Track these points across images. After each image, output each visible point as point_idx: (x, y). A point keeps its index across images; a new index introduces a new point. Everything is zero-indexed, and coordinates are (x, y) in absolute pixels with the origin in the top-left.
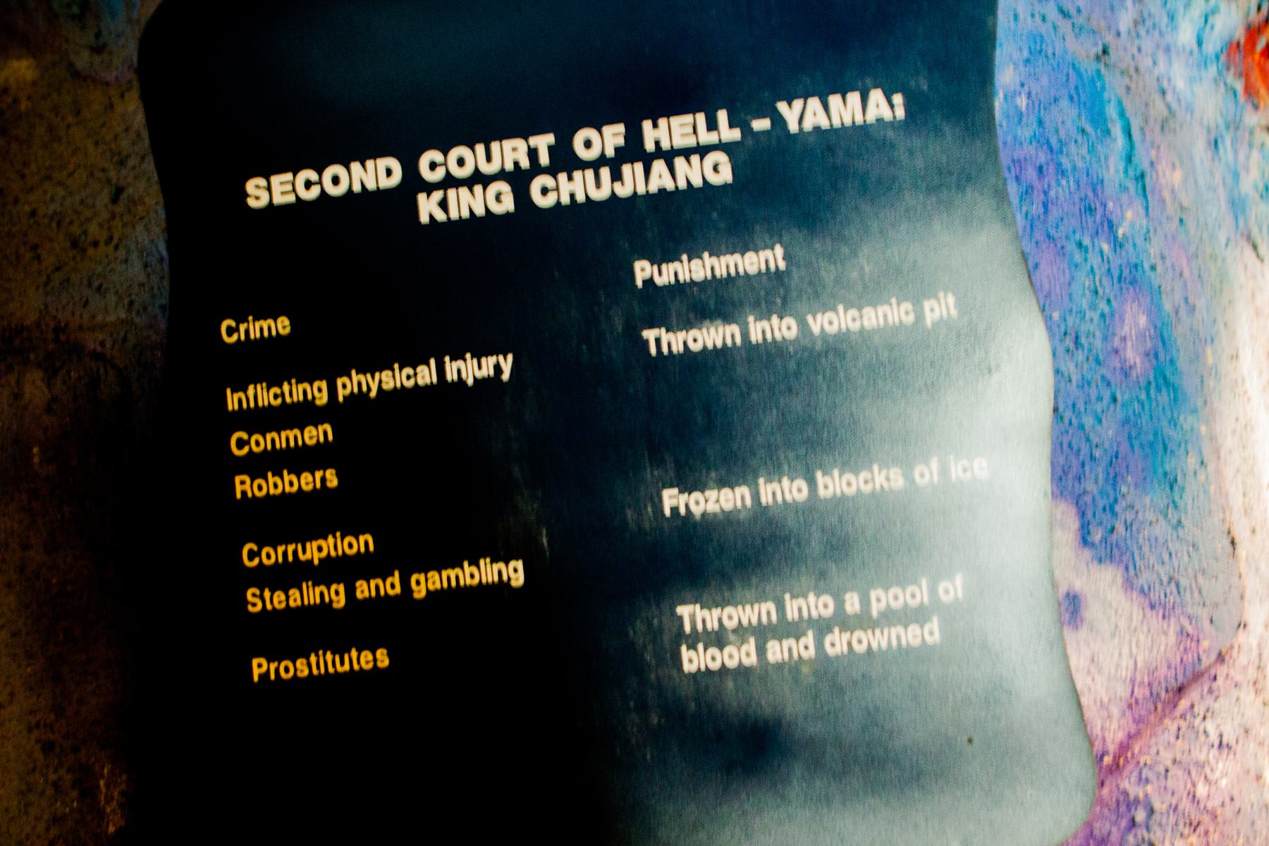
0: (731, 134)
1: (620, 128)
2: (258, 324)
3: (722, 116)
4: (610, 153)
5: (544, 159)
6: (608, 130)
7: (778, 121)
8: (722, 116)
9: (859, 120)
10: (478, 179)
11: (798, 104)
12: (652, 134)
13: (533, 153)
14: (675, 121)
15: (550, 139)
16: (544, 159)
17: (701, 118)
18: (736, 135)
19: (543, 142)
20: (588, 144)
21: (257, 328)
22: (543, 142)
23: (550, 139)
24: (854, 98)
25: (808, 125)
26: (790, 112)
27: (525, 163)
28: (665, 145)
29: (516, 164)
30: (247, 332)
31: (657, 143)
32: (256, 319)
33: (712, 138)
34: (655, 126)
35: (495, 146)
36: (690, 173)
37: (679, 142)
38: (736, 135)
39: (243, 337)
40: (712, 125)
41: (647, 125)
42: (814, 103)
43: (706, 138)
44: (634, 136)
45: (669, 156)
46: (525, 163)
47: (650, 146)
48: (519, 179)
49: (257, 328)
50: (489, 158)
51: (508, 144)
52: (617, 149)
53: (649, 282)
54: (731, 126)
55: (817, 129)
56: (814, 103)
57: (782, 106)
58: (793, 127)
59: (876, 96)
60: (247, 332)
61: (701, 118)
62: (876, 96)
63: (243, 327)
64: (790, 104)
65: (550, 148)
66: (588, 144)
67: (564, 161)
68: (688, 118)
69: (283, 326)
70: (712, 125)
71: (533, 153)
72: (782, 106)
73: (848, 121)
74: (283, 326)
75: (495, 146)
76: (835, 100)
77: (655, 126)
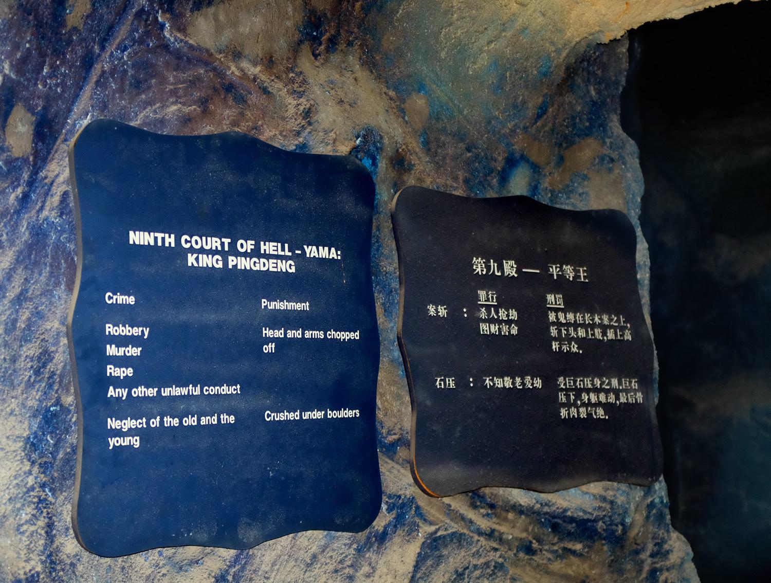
1: (253, 242)
4: (249, 251)
5: (226, 249)
6: (249, 242)
7: (304, 252)
13: (222, 244)
14: (272, 244)
15: (229, 240)
16: (226, 249)
17: (279, 245)
19: (227, 241)
22: (227, 241)
23: (229, 240)
24: (326, 249)
25: (312, 256)
27: (219, 248)
31: (265, 250)
33: (283, 253)
38: (290, 254)
40: (283, 250)
42: (314, 248)
44: (257, 247)
47: (262, 252)
51: (214, 239)
52: (251, 249)
54: (289, 251)
66: (242, 246)
68: (275, 244)
70: (283, 250)
71: (222, 244)
72: (305, 247)
76: (321, 248)
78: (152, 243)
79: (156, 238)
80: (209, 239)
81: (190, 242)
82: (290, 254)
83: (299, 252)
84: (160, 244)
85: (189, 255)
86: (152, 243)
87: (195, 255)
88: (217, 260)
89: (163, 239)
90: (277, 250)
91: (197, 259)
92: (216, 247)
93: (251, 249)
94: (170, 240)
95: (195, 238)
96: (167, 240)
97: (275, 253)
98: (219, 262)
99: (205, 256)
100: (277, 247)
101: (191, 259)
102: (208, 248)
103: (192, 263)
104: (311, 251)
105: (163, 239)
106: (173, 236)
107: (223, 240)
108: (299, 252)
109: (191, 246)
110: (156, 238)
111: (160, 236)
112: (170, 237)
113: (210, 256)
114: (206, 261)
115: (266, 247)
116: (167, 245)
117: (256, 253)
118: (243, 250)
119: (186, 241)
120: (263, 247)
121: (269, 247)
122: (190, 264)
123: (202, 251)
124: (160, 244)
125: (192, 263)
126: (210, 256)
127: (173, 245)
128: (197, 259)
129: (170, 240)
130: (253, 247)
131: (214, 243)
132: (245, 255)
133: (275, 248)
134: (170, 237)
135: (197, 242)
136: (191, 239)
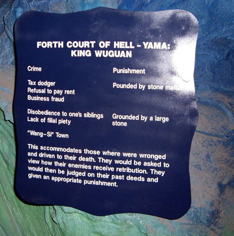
0: (132, 47)
1: (109, 42)
2: (35, 68)
3: (131, 43)
4: (106, 47)
5: (93, 46)
6: (107, 42)
7: (143, 46)
8: (131, 43)
11: (147, 43)
12: (115, 45)
13: (90, 45)
14: (121, 42)
15: (95, 42)
16: (93, 46)
17: (126, 43)
18: (133, 47)
19: (93, 43)
20: (102, 45)
21: (35, 69)
22: (93, 43)
23: (95, 42)
24: (159, 43)
25: (149, 48)
26: (145, 44)
27: (89, 47)
28: (118, 47)
29: (87, 46)
30: (33, 69)
31: (117, 46)
32: (35, 67)
33: (128, 47)
34: (117, 43)
35: (83, 42)
36: (122, 54)
37: (121, 47)
38: (133, 47)
40: (129, 45)
41: (115, 42)
43: (127, 47)
44: (112, 44)
47: (115, 47)
49: (35, 69)
50: (81, 45)
51: (86, 42)
52: (108, 46)
54: (133, 46)
55: (150, 49)
56: (151, 43)
57: (144, 43)
58: (145, 47)
59: (164, 44)
60: (33, 69)
61: (126, 43)
62: (164, 44)
63: (32, 68)
64: (146, 43)
65: (94, 44)
66: (102, 45)
68: (124, 42)
69: (40, 69)
70: (129, 45)
71: (90, 45)
72: (144, 43)
73: (157, 48)
74: (40, 69)
75: (83, 42)
76: (155, 43)
77: (117, 43)
78: (51, 47)
79: (53, 45)
81: (72, 44)
83: (140, 46)
84: (55, 46)
85: (72, 51)
86: (51, 47)
87: (75, 51)
88: (88, 53)
89: (57, 44)
90: (125, 46)
91: (76, 53)
92: (87, 46)
93: (108, 46)
94: (61, 44)
95: (74, 42)
97: (124, 47)
98: (89, 53)
99: (81, 51)
100: (125, 44)
101: (73, 53)
103: (74, 55)
105: (57, 44)
106: (62, 42)
108: (140, 46)
109: (72, 46)
110: (53, 45)
111: (55, 43)
112: (61, 43)
113: (84, 51)
114: (81, 53)
115: (118, 45)
116: (59, 47)
117: (111, 48)
118: (103, 47)
119: (70, 44)
120: (115, 45)
122: (72, 55)
123: (78, 48)
124: (55, 46)
125: (74, 55)
127: (62, 47)
128: (76, 53)
129: (61, 44)
130: (109, 45)
132: (104, 49)
133: (124, 45)
134: (61, 43)
135: (77, 44)
136: (72, 43)
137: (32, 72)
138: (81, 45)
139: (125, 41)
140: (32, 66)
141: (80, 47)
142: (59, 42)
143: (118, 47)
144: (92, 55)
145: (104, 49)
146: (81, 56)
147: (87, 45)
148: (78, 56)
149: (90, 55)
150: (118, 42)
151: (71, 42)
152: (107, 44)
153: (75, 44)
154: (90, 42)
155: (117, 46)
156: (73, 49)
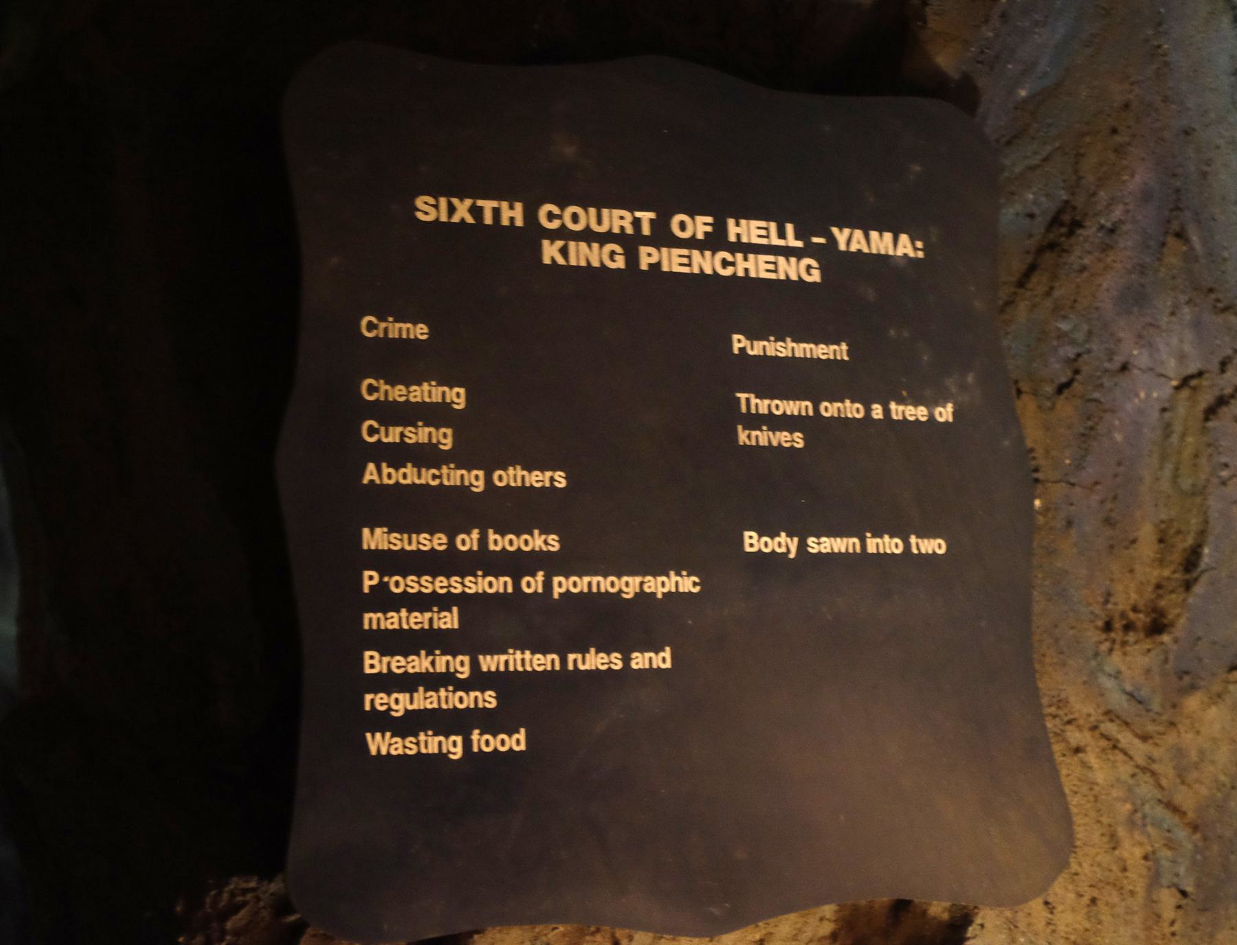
0: (793, 242)
1: (709, 219)
2: (398, 325)
3: (790, 228)
4: (700, 236)
5: (646, 230)
6: (700, 219)
7: (832, 240)
8: (790, 228)
9: (891, 253)
10: (588, 236)
12: (733, 230)
13: (637, 223)
14: (755, 223)
16: (646, 230)
19: (646, 216)
23: (652, 215)
24: (888, 236)
25: (853, 248)
26: (841, 236)
27: (629, 230)
30: (386, 330)
33: (781, 243)
34: (738, 225)
36: (758, 267)
38: (799, 244)
39: (381, 335)
40: (782, 234)
43: (776, 241)
45: (749, 249)
46: (629, 230)
47: (732, 238)
48: (630, 243)
50: (599, 222)
51: (617, 213)
53: (742, 350)
57: (835, 230)
58: (842, 247)
59: (904, 238)
60: (386, 330)
62: (904, 238)
63: (383, 325)
64: (841, 230)
66: (683, 226)
67: (662, 237)
68: (763, 224)
70: (782, 234)
71: (637, 223)
72: (835, 230)
76: (874, 235)
77: (738, 225)
80: (605, 212)
81: (560, 217)
82: (799, 244)
85: (546, 243)
87: (560, 243)
90: (767, 237)
91: (564, 251)
92: (622, 228)
93: (706, 233)
94: (513, 214)
96: (506, 215)
97: (764, 241)
99: (583, 245)
101: (550, 252)
102: (603, 229)
103: (553, 259)
104: (849, 239)
106: (519, 206)
107: (638, 214)
112: (512, 207)
114: (583, 255)
117: (715, 241)
119: (551, 216)
120: (733, 230)
121: (749, 230)
123: (588, 236)
126: (595, 246)
128: (564, 251)
129: (513, 214)
130: (709, 229)
131: (617, 219)
132: (692, 243)
134: (512, 207)
137: (386, 343)
138: (599, 222)
139: (767, 219)
140: (382, 319)
141: (596, 228)
142: (505, 205)
143: (744, 240)
144: (627, 262)
145: (692, 243)
146: (583, 263)
147: (623, 223)
148: (573, 262)
149: (620, 263)
150: (743, 222)
151: (556, 210)
152: (701, 226)
153: (575, 218)
154: (633, 214)
155: (738, 235)
156: (553, 235)
